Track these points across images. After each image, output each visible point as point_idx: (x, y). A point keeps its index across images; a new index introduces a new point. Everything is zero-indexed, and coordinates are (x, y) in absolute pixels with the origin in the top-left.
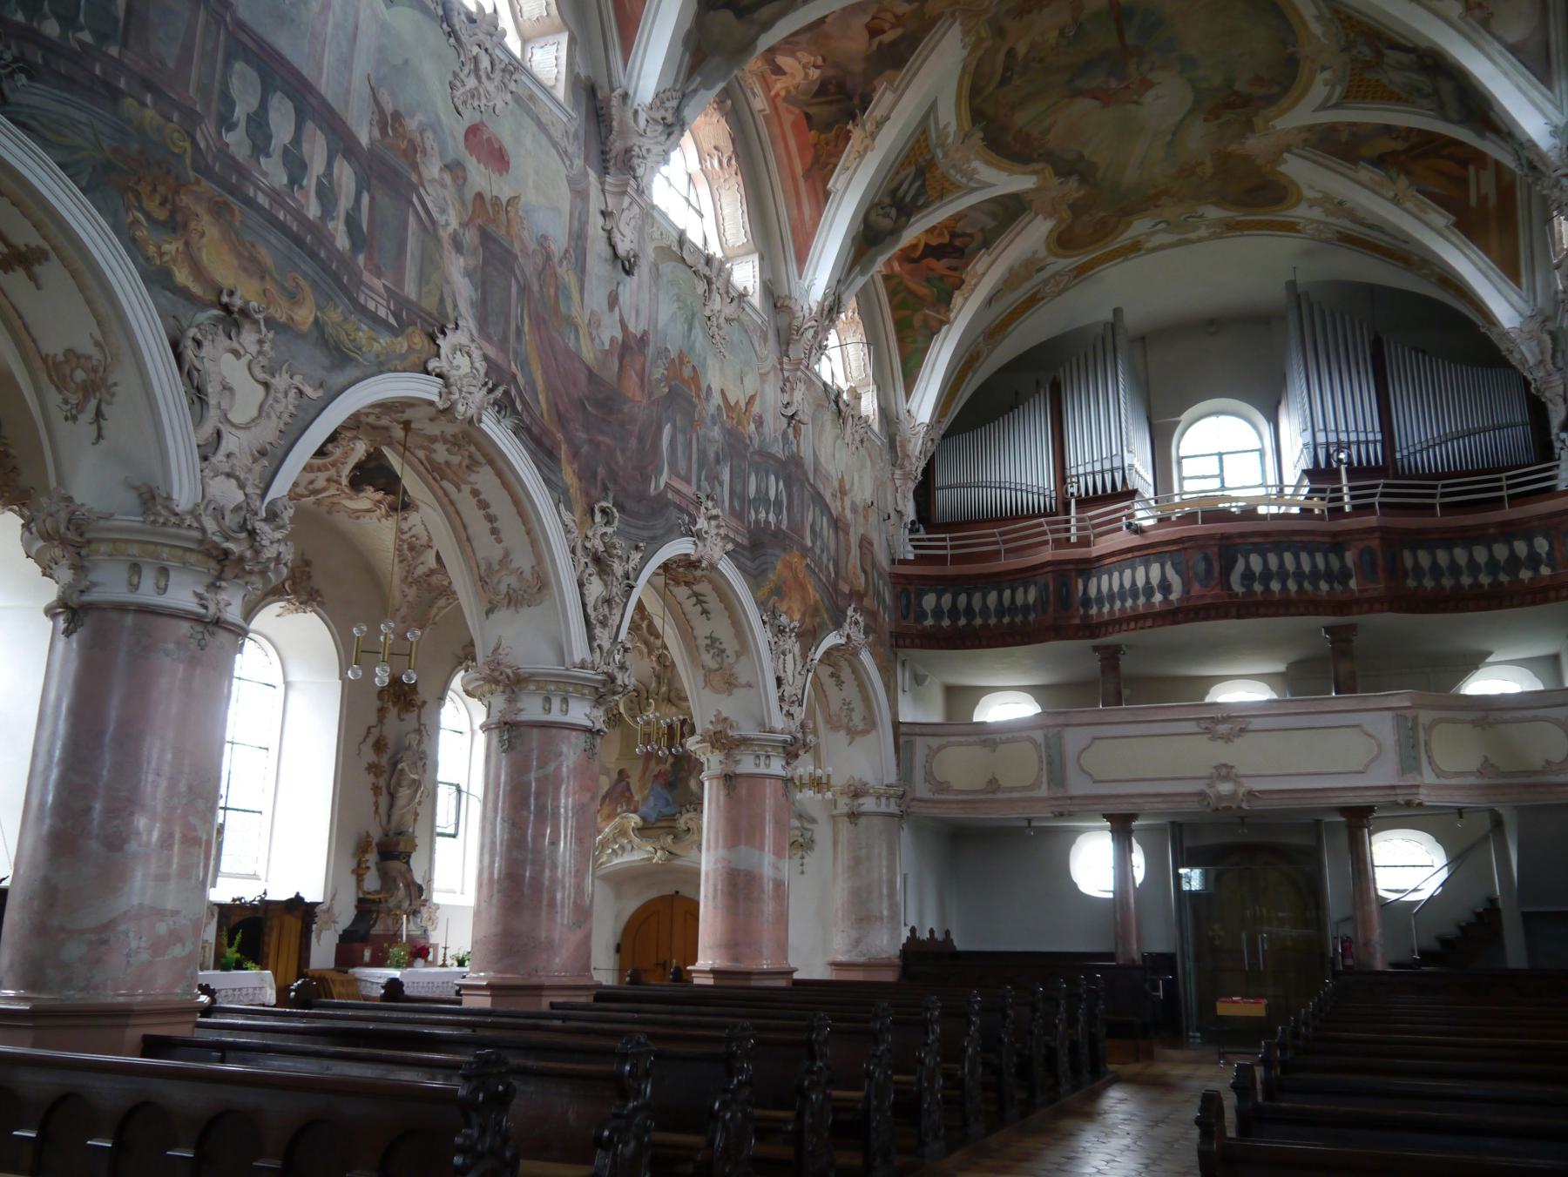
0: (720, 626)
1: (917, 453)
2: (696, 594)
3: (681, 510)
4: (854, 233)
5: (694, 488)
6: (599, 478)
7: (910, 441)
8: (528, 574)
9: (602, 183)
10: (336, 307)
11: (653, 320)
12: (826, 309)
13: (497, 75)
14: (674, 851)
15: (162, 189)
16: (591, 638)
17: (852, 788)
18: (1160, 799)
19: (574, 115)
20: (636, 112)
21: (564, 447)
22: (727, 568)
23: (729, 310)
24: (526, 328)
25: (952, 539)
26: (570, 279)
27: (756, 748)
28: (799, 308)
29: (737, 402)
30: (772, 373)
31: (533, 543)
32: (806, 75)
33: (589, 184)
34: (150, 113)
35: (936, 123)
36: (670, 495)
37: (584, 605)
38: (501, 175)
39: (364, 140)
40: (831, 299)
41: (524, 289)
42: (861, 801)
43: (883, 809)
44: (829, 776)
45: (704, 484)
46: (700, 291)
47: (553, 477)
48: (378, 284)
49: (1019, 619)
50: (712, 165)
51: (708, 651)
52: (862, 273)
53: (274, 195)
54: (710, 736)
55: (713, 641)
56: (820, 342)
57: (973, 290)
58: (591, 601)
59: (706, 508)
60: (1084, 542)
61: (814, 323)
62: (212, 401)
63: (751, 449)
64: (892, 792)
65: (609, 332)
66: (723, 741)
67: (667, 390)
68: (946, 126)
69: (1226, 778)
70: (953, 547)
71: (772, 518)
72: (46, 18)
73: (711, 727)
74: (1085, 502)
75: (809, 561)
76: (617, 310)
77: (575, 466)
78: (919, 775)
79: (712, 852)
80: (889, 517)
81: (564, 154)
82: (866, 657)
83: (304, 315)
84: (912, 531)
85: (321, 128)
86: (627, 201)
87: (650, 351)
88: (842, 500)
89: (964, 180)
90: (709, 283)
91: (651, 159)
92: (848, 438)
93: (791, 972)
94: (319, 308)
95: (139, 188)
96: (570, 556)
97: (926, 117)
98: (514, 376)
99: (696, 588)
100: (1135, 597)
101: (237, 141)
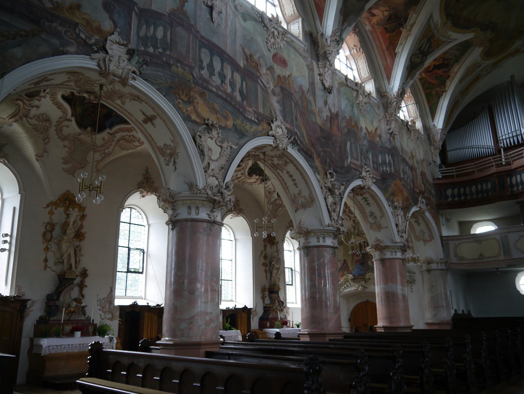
0: (374, 208)
1: (439, 139)
2: (364, 198)
3: (356, 170)
4: (407, 66)
5: (360, 162)
6: (327, 163)
7: (435, 136)
8: (307, 197)
9: (318, 65)
10: (239, 119)
11: (340, 107)
12: (400, 94)
13: (280, 36)
14: (366, 286)
15: (185, 91)
16: (330, 216)
17: (427, 261)
19: (306, 44)
20: (326, 39)
21: (315, 154)
22: (374, 188)
23: (365, 100)
24: (298, 117)
25: (455, 169)
26: (311, 98)
27: (391, 249)
28: (389, 95)
29: (372, 131)
30: (383, 120)
31: (308, 187)
32: (383, 14)
33: (313, 66)
34: (180, 69)
35: (433, 21)
36: (352, 165)
37: (327, 206)
38: (285, 68)
39: (242, 65)
40: (401, 90)
41: (296, 104)
42: (431, 265)
43: (440, 267)
44: (418, 257)
45: (363, 160)
46: (354, 95)
47: (312, 164)
48: (251, 110)
49: (485, 195)
50: (354, 52)
51: (370, 217)
52: (411, 79)
53: (217, 87)
54: (374, 246)
55: (372, 214)
56: (399, 106)
57: (454, 78)
58: (329, 204)
59: (365, 169)
60: (508, 164)
61: (395, 99)
62: (206, 154)
63: (378, 146)
64: (442, 261)
65: (326, 113)
66: (379, 247)
67: (347, 130)
68: (437, 22)
70: (456, 172)
71: (388, 169)
72: (149, 47)
73: (374, 243)
74: (507, 149)
75: (403, 182)
76: (327, 106)
77: (319, 160)
78: (452, 254)
79: (379, 286)
80: (431, 164)
81: (304, 58)
82: (427, 214)
83: (230, 123)
84: (440, 168)
85: (229, 64)
86: (327, 69)
87: (340, 118)
88: (413, 160)
89: (446, 40)
90: (357, 91)
91: (333, 55)
92: (412, 138)
93: (412, 327)
94: (234, 120)
96: (321, 190)
97: (429, 20)
98: (296, 133)
99: (364, 196)
101: (205, 73)
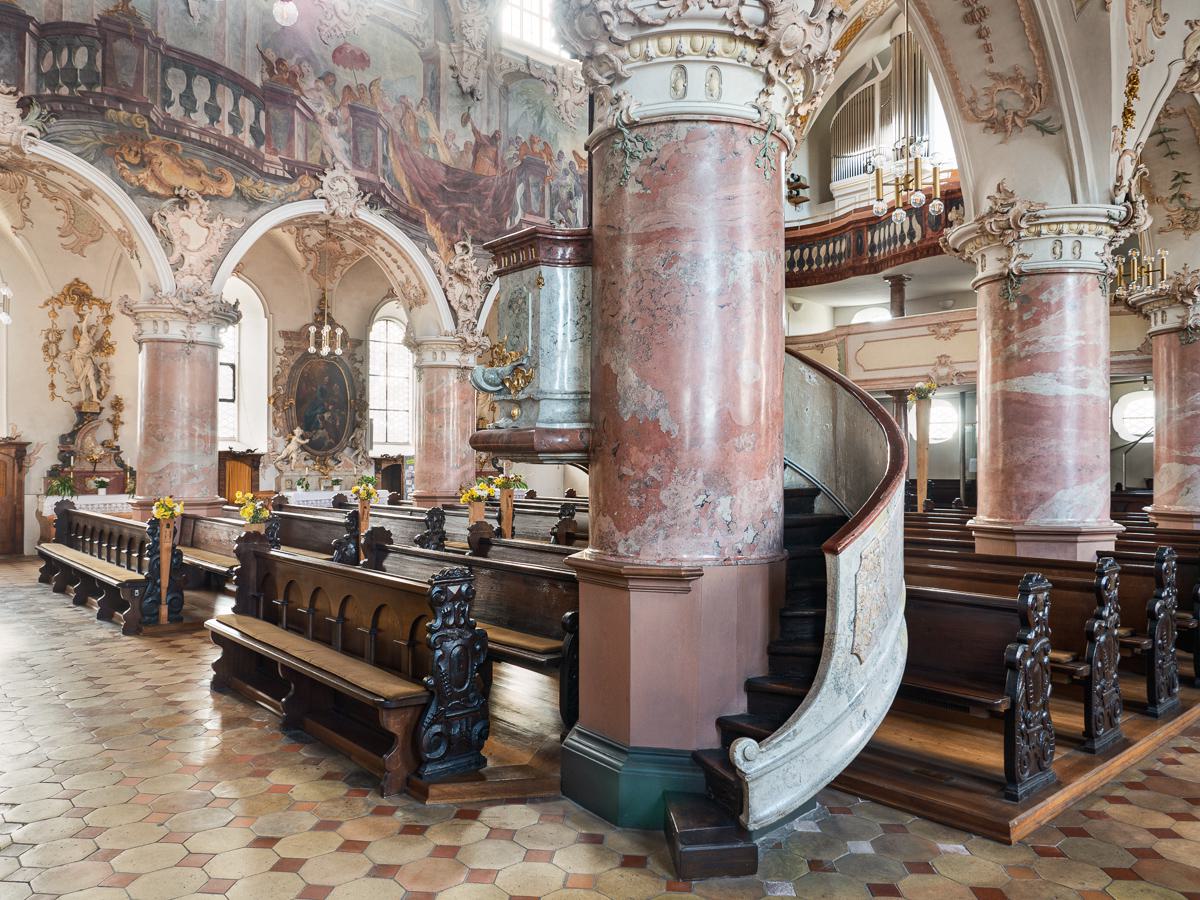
5: (548, 218)
6: (459, 229)
10: (248, 178)
18: (903, 381)
38: (363, 69)
39: (258, 83)
41: (386, 134)
48: (276, 159)
53: (202, 131)
62: (176, 243)
69: (944, 365)
72: (61, 86)
76: (469, 124)
83: (228, 188)
85: (228, 86)
94: (237, 181)
95: (122, 152)
98: (383, 185)
100: (902, 239)
